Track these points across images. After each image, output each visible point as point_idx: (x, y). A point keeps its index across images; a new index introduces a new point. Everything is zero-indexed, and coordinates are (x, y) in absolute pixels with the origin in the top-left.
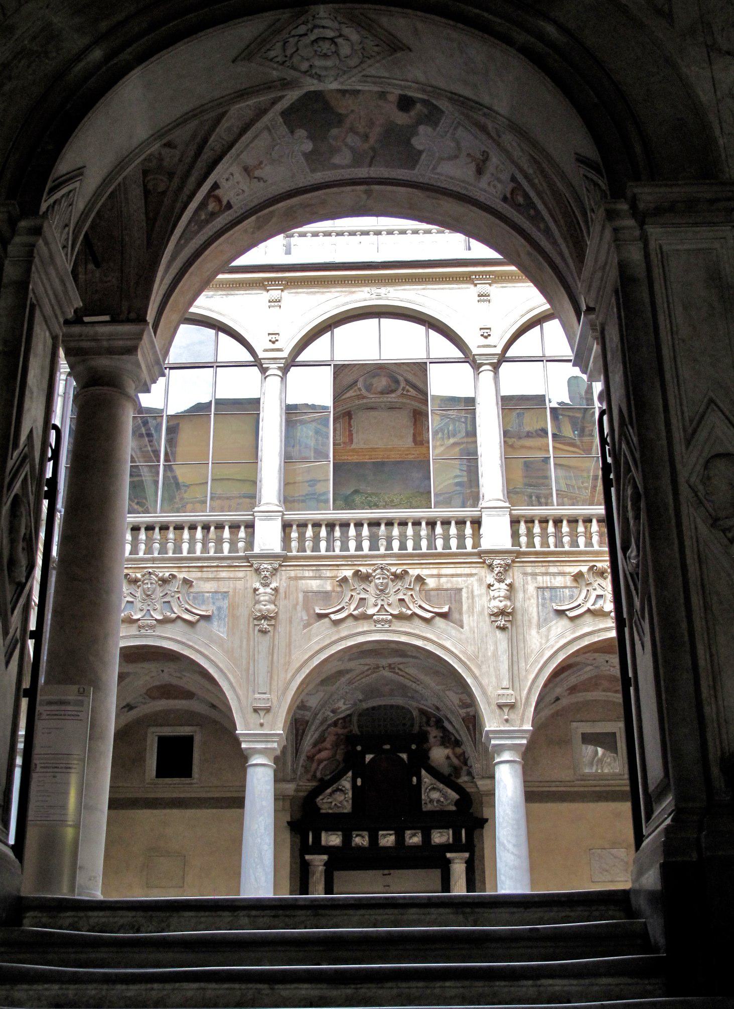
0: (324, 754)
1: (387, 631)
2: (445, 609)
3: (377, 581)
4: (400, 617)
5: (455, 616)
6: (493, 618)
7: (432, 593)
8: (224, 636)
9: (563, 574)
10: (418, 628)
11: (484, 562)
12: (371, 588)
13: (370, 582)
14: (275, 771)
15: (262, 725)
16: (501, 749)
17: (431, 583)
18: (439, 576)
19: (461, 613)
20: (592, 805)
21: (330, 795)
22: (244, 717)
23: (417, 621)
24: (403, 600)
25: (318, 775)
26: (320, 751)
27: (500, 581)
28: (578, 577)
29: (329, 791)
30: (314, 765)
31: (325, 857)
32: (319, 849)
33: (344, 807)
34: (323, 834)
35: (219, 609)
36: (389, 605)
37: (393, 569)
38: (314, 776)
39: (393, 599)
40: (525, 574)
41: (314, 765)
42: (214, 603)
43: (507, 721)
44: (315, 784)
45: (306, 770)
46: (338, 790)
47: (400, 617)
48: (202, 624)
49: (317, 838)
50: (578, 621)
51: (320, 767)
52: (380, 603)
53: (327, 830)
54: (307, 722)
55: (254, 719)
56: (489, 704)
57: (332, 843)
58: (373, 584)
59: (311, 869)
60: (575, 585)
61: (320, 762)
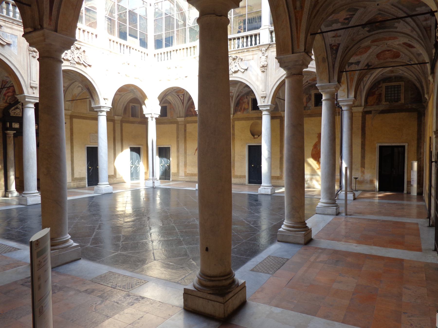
0: (10, 94)
1: (74, 67)
4: (78, 63)
8: (17, 54)
10: (82, 67)
14: (35, 109)
15: (34, 93)
20: (91, 121)
21: (14, 109)
22: (27, 89)
23: (83, 66)
24: (78, 57)
25: (8, 101)
26: (8, 93)
29: (13, 108)
30: (6, 98)
31: (15, 132)
32: (11, 129)
33: (19, 114)
34: (13, 124)
35: (14, 42)
38: (6, 102)
39: (76, 56)
41: (6, 98)
42: (11, 39)
44: (7, 104)
45: (3, 99)
46: (17, 108)
47: (78, 63)
48: (7, 47)
49: (11, 125)
51: (9, 98)
52: (72, 56)
53: (14, 122)
54: (7, 82)
55: (30, 90)
57: (16, 127)
59: (7, 135)
61: (8, 96)
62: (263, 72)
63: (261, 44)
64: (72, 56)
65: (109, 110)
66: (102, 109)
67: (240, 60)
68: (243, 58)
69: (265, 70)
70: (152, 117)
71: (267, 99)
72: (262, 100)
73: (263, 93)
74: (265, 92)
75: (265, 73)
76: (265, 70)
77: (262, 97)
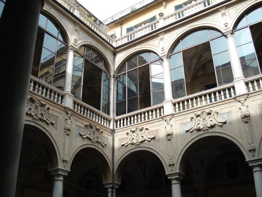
2: (54, 122)
3: (37, 104)
5: (55, 125)
6: (66, 131)
7: (50, 115)
9: (83, 123)
11: (65, 111)
12: (34, 105)
13: (34, 103)
16: (59, 175)
17: (51, 111)
18: (53, 110)
19: (57, 125)
27: (70, 119)
28: (86, 126)
36: (38, 114)
37: (42, 102)
39: (40, 112)
40: (74, 119)
43: (64, 166)
50: (84, 139)
52: (35, 112)
56: (60, 159)
58: (34, 104)
60: (85, 128)
62: (247, 122)
63: (238, 94)
64: (35, 112)
65: (67, 174)
66: (60, 173)
67: (215, 114)
68: (219, 111)
69: (249, 120)
70: (112, 188)
71: (257, 152)
72: (251, 154)
73: (251, 145)
74: (253, 145)
75: (249, 123)
76: (249, 120)
77: (250, 151)
